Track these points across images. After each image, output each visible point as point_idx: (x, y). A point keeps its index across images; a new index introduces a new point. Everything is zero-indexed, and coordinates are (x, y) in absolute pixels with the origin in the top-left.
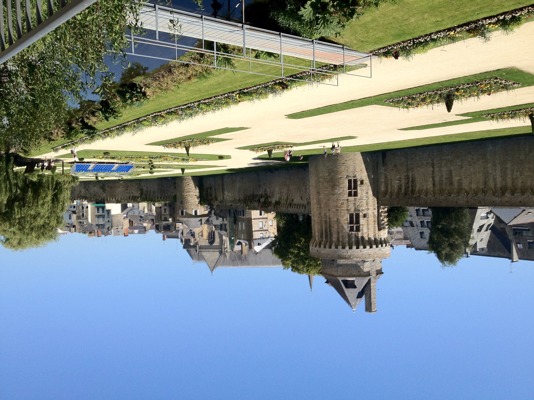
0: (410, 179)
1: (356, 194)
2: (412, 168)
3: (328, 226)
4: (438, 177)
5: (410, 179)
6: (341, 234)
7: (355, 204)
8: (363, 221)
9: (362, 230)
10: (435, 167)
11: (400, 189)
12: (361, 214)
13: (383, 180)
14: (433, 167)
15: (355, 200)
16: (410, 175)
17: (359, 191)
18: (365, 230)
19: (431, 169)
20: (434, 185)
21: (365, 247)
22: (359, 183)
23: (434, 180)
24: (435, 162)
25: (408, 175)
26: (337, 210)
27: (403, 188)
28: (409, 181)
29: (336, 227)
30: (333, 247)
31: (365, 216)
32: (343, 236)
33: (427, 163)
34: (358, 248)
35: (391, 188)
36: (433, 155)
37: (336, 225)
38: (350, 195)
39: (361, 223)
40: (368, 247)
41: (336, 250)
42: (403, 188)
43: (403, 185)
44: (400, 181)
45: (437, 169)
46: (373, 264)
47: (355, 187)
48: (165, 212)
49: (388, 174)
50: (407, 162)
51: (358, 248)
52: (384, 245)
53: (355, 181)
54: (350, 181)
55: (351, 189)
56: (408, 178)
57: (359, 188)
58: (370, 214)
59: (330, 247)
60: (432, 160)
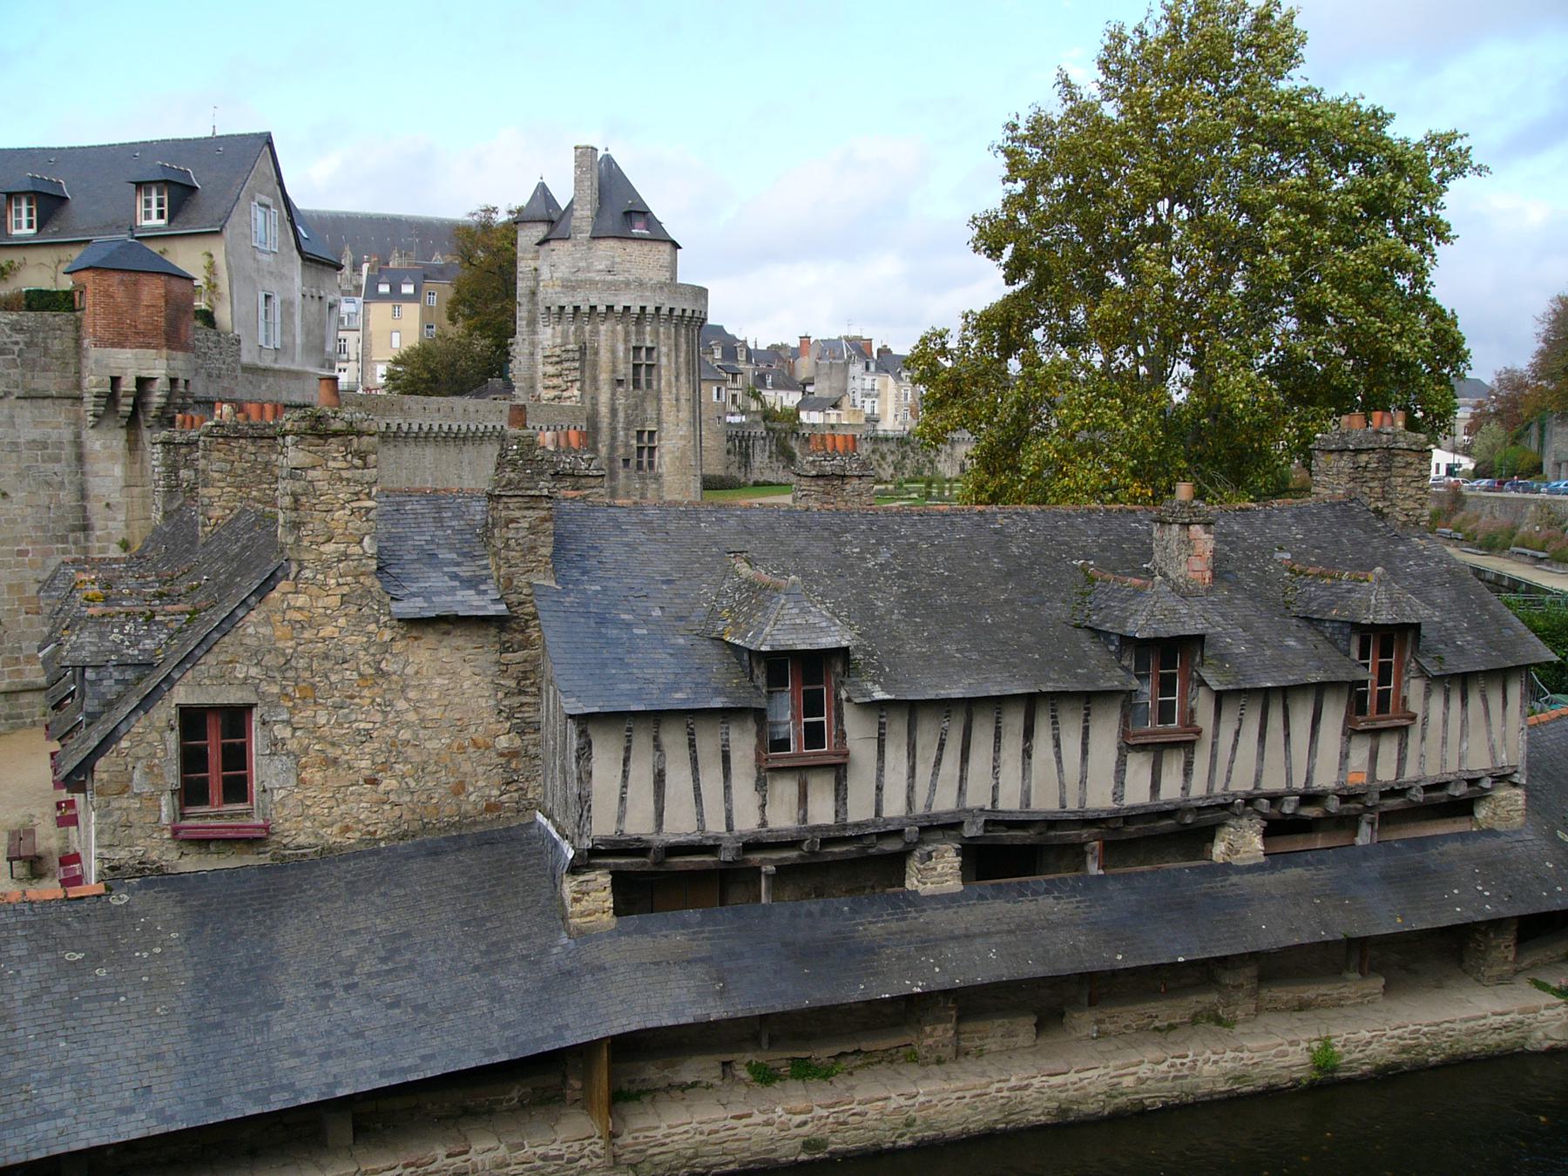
1: (640, 433)
6: (672, 342)
9: (627, 350)
17: (634, 442)
18: (621, 348)
21: (627, 308)
22: (633, 462)
31: (620, 382)
34: (643, 308)
38: (652, 433)
40: (619, 308)
46: (582, 264)
47: (640, 449)
48: (734, 396)
51: (643, 308)
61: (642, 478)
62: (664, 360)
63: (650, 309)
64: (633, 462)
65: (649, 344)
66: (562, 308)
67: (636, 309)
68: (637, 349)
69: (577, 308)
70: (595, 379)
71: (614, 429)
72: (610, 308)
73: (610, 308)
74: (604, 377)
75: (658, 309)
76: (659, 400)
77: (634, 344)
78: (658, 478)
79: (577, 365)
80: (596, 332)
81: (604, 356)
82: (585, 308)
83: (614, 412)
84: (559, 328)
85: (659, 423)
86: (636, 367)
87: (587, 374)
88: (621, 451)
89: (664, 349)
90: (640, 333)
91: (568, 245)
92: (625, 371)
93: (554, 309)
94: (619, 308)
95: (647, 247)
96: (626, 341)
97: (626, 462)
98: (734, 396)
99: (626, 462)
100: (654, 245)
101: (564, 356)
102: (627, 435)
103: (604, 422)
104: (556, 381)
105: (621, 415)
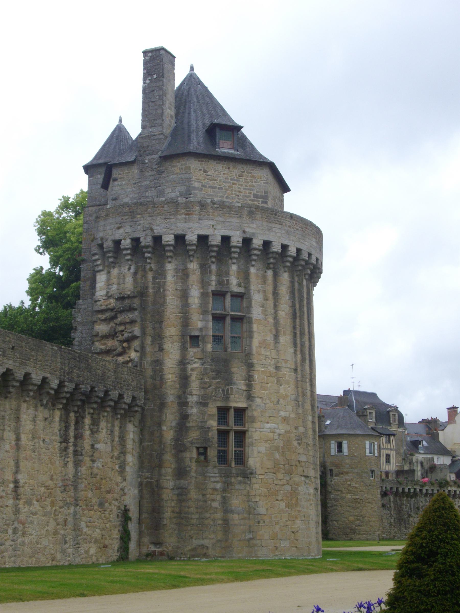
0: (71, 449)
1: (223, 412)
2: (65, 488)
3: (298, 320)
4: (7, 447)
5: (71, 449)
6: (270, 289)
7: (229, 381)
8: (200, 325)
9: (204, 295)
10: (12, 485)
11: (95, 423)
12: (209, 347)
13: (130, 459)
14: (16, 482)
15: (227, 398)
16: (71, 465)
17: (213, 423)
19: (22, 478)
20: (18, 419)
21: (203, 239)
22: (212, 453)
23: (18, 439)
24: (11, 502)
25: (77, 464)
26: (277, 368)
27: (87, 421)
28: (75, 445)
29: (281, 314)
30: (292, 251)
32: (264, 282)
33: (29, 503)
34: (226, 239)
35: (113, 426)
36: (15, 531)
37: (282, 322)
38: (240, 413)
39: (210, 318)
40: (192, 238)
41: (286, 242)
42: (87, 421)
43: (88, 433)
44: (93, 446)
45: (9, 476)
48: (388, 456)
49: (119, 479)
50: (75, 513)
51: (226, 239)
52: (126, 243)
53: (223, 458)
54: (241, 459)
55: (236, 432)
56: (76, 452)
57: (213, 435)
58: (177, 346)
59: (299, 251)
60: (17, 511)
61: (227, 475)
62: (256, 313)
63: (237, 240)
64: (212, 453)
65: (236, 289)
66: (117, 243)
67: (216, 240)
68: (219, 295)
69: (136, 241)
70: (159, 338)
71: (183, 403)
72: (180, 239)
73: (180, 239)
74: (171, 331)
75: (247, 241)
76: (250, 366)
77: (213, 287)
78: (247, 475)
79: (135, 315)
80: (160, 274)
81: (172, 303)
82: (146, 241)
83: (184, 379)
84: (115, 272)
85: (250, 397)
86: (219, 319)
87: (149, 330)
88: (194, 435)
89: (257, 298)
90: (223, 275)
91: (135, 170)
92: (200, 323)
93: (108, 244)
94: (192, 238)
95: (236, 170)
96: (204, 284)
97: (203, 451)
98: (388, 456)
99: (203, 451)
100: (247, 169)
101: (120, 305)
102: (203, 413)
103: (171, 394)
104: (110, 343)
105: (195, 385)
